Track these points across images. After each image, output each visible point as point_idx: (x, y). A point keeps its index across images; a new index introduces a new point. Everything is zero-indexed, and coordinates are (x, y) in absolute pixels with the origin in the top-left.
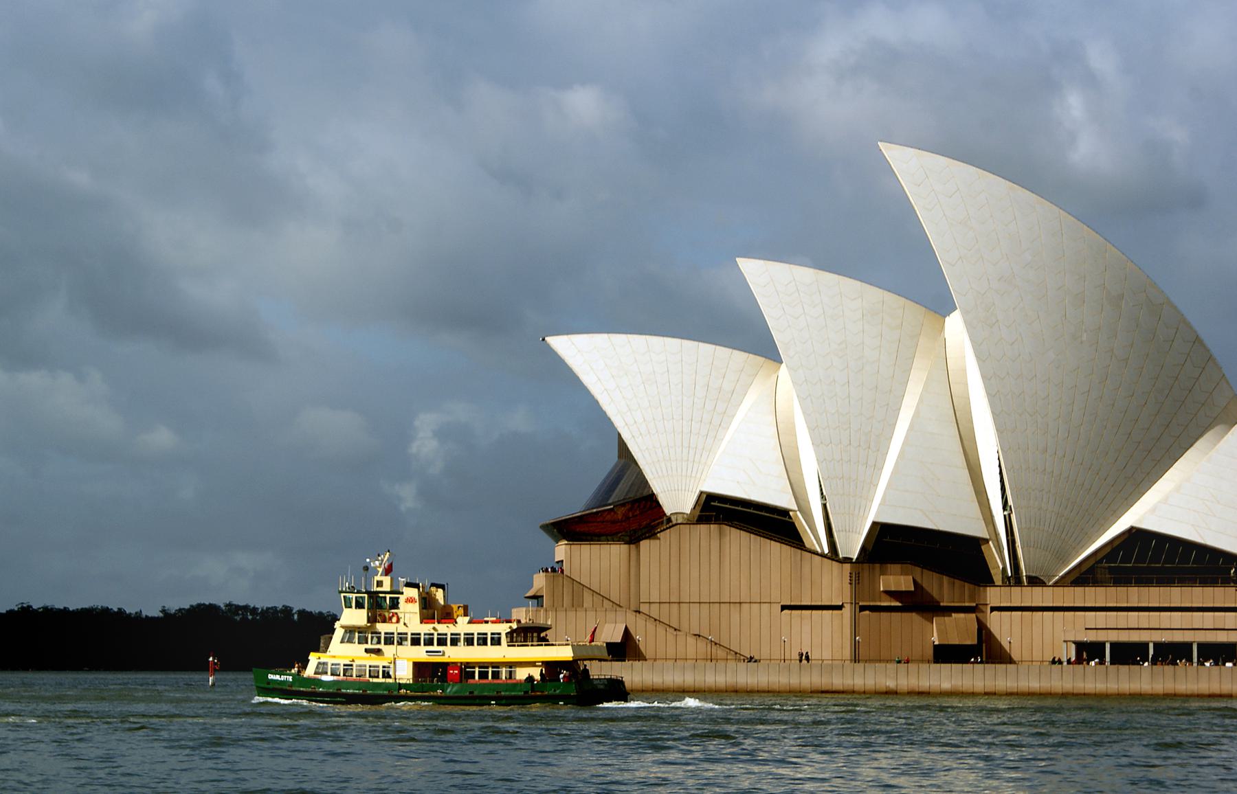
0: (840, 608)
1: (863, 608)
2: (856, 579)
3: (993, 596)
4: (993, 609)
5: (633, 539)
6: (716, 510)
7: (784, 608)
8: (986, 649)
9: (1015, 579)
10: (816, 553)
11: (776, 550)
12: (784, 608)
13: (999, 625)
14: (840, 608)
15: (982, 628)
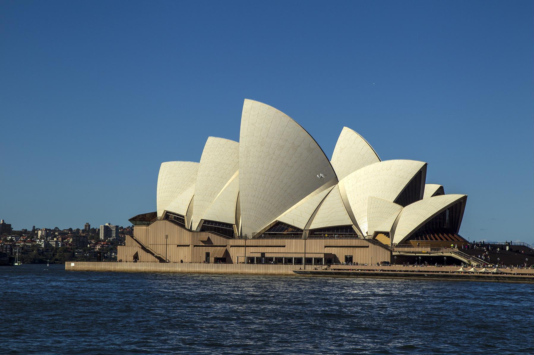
0: (189, 246)
1: (195, 246)
2: (193, 237)
3: (231, 242)
4: (231, 246)
5: (148, 225)
6: (168, 216)
7: (178, 246)
8: (225, 259)
9: (241, 237)
10: (186, 229)
11: (177, 227)
12: (178, 246)
13: (233, 252)
14: (189, 246)
15: (227, 253)
